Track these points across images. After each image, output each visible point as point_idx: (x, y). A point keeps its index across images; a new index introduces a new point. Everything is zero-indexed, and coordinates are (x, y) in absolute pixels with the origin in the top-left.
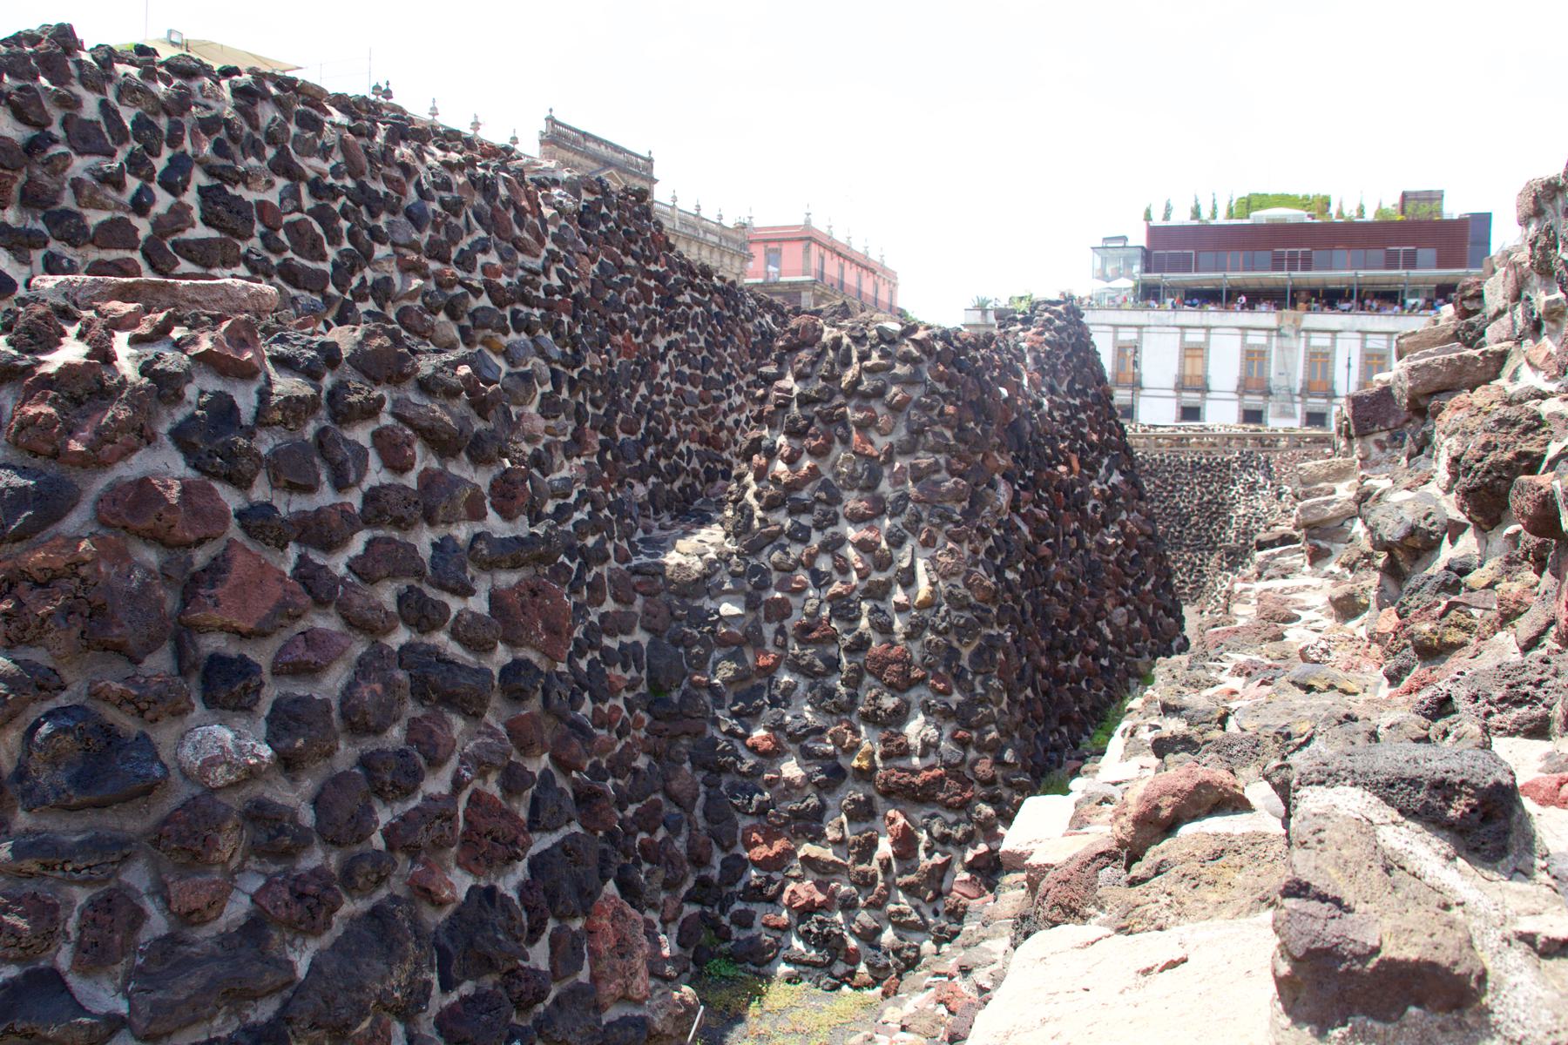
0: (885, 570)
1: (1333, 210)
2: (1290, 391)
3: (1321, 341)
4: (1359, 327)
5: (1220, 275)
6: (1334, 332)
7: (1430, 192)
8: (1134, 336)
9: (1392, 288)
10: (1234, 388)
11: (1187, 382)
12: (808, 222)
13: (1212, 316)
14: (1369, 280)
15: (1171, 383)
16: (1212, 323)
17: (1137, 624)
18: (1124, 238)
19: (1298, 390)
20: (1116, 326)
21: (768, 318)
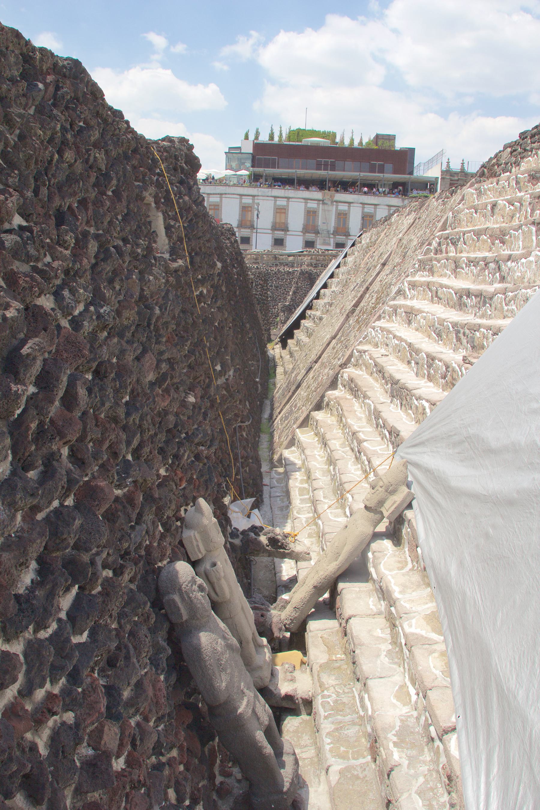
1: (338, 140)
2: (328, 232)
3: (343, 207)
5: (294, 171)
6: (350, 203)
8: (250, 201)
9: (373, 182)
10: (301, 229)
11: (278, 226)
13: (289, 192)
14: (364, 178)
15: (270, 227)
16: (291, 196)
18: (239, 148)
19: (332, 232)
20: (241, 195)
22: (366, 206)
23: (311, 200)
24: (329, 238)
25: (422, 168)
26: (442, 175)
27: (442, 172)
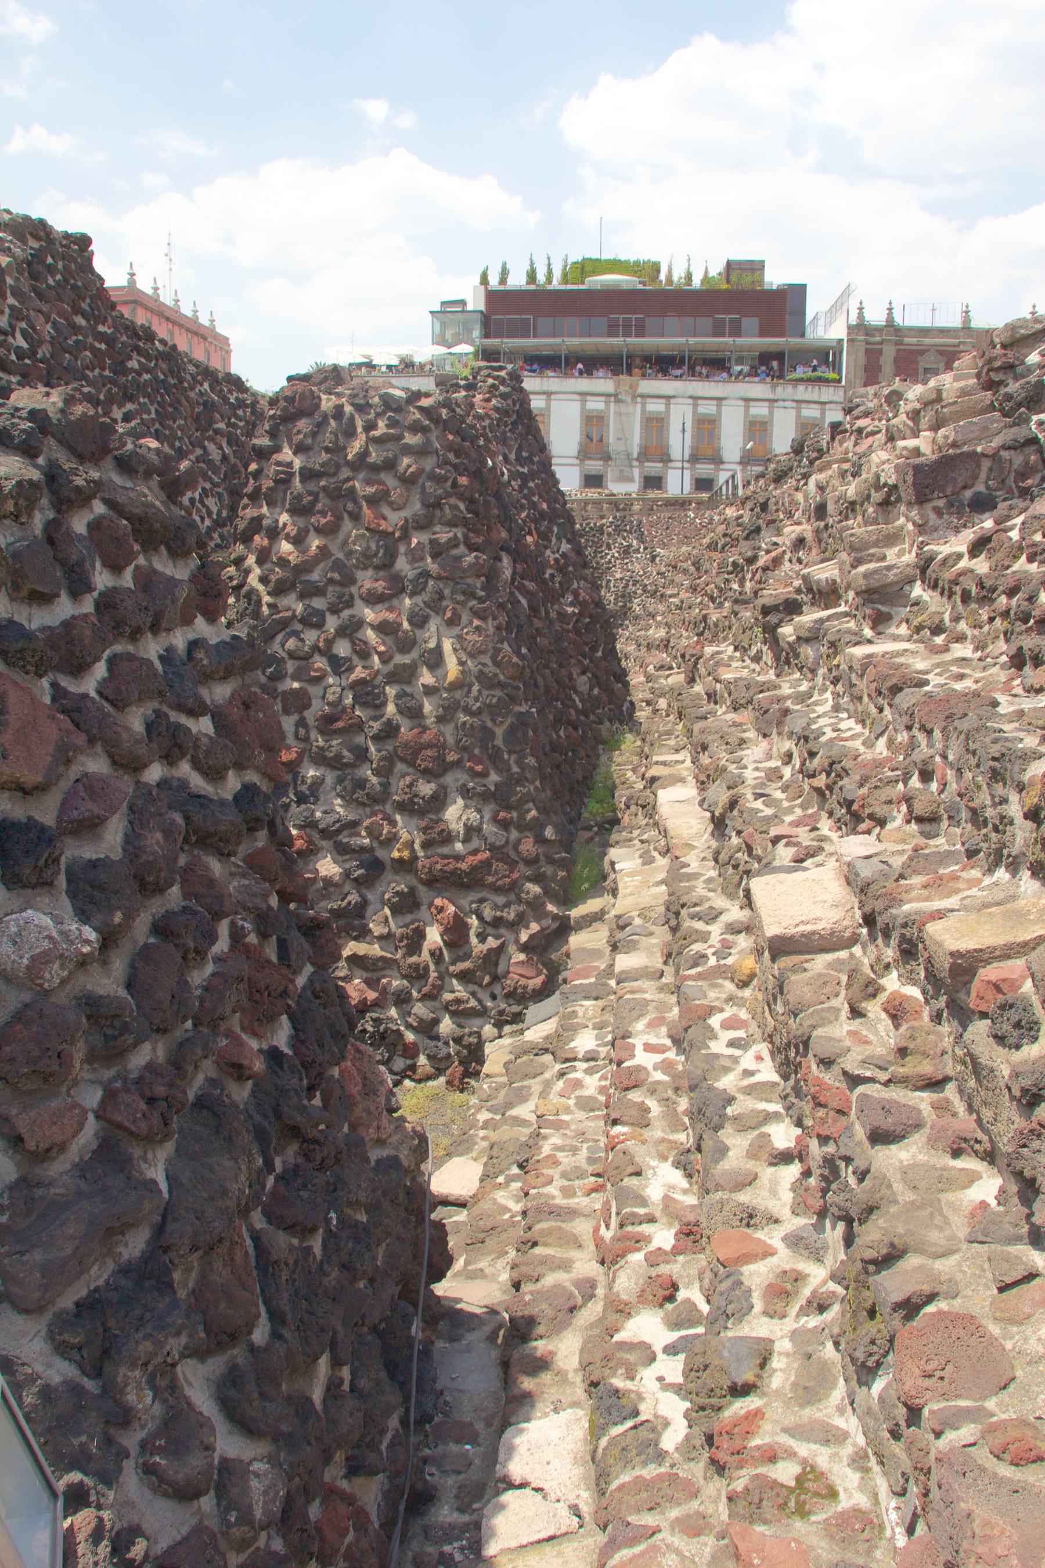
0: (409, 652)
1: (662, 277)
2: (628, 455)
3: (655, 407)
4: (691, 392)
5: (558, 340)
6: (668, 398)
7: (752, 262)
9: (720, 355)
10: (575, 453)
12: (132, 283)
14: (698, 348)
16: (553, 389)
17: (596, 691)
18: (463, 303)
19: (635, 455)
21: (206, 386)
22: (700, 402)
23: (593, 395)
24: (631, 466)
25: (821, 322)
26: (849, 334)
27: (849, 327)
